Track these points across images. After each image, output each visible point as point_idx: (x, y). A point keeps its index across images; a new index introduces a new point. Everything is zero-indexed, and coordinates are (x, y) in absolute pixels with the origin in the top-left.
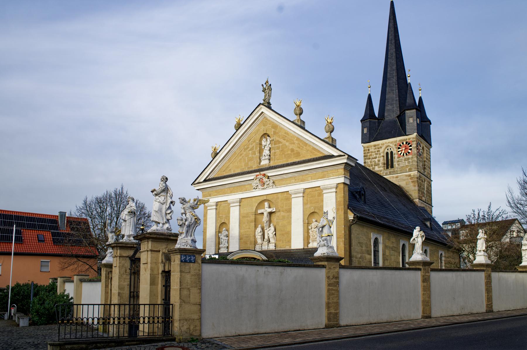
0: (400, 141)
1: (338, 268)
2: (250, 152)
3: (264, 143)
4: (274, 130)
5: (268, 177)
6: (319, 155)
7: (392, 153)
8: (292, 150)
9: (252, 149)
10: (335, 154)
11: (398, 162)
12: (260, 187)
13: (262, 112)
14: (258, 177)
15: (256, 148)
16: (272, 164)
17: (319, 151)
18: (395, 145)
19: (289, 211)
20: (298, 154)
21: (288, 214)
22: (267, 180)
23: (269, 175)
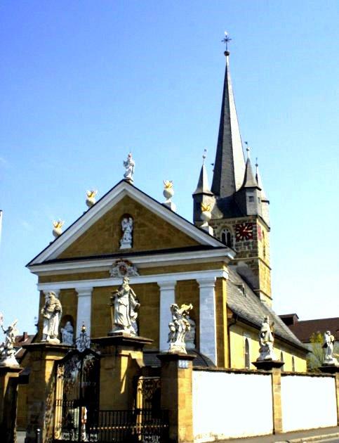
0: (239, 221)
1: (280, 375)
2: (107, 233)
3: (124, 226)
4: (138, 211)
5: (132, 265)
6: (193, 244)
7: (229, 234)
8: (161, 236)
9: (108, 230)
10: (215, 245)
11: (236, 246)
12: (120, 275)
13: (124, 190)
14: (119, 263)
15: (114, 229)
16: (135, 250)
17: (193, 240)
18: (234, 226)
19: (158, 305)
20: (168, 241)
21: (155, 308)
22: (129, 267)
23: (134, 262)
